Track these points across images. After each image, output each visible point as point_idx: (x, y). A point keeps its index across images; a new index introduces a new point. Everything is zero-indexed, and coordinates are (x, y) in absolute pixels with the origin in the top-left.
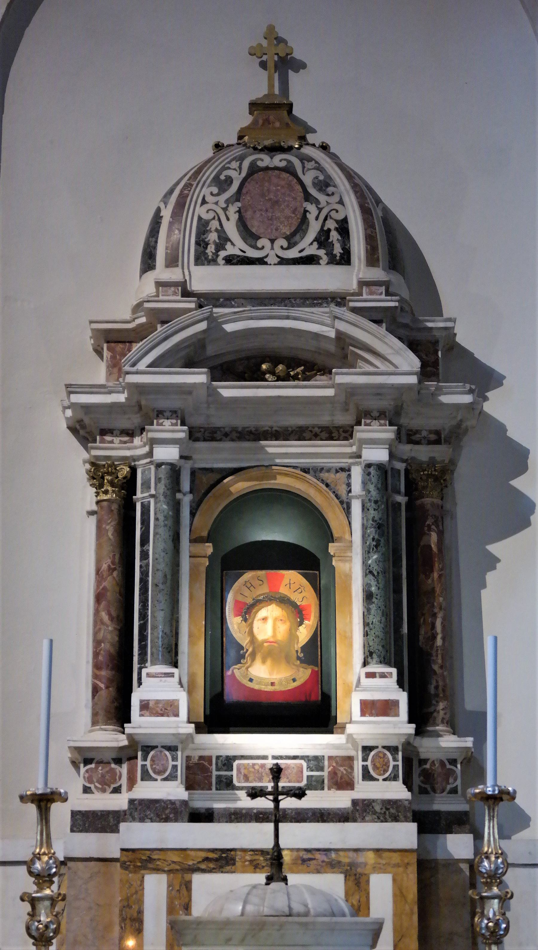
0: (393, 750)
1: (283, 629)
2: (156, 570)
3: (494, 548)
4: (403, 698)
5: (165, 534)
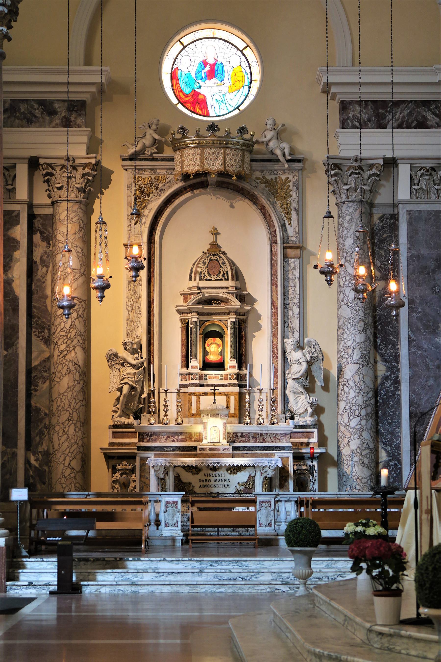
0: (235, 374)
1: (216, 349)
2: (193, 341)
3: (255, 334)
4: (237, 365)
5: (195, 335)
